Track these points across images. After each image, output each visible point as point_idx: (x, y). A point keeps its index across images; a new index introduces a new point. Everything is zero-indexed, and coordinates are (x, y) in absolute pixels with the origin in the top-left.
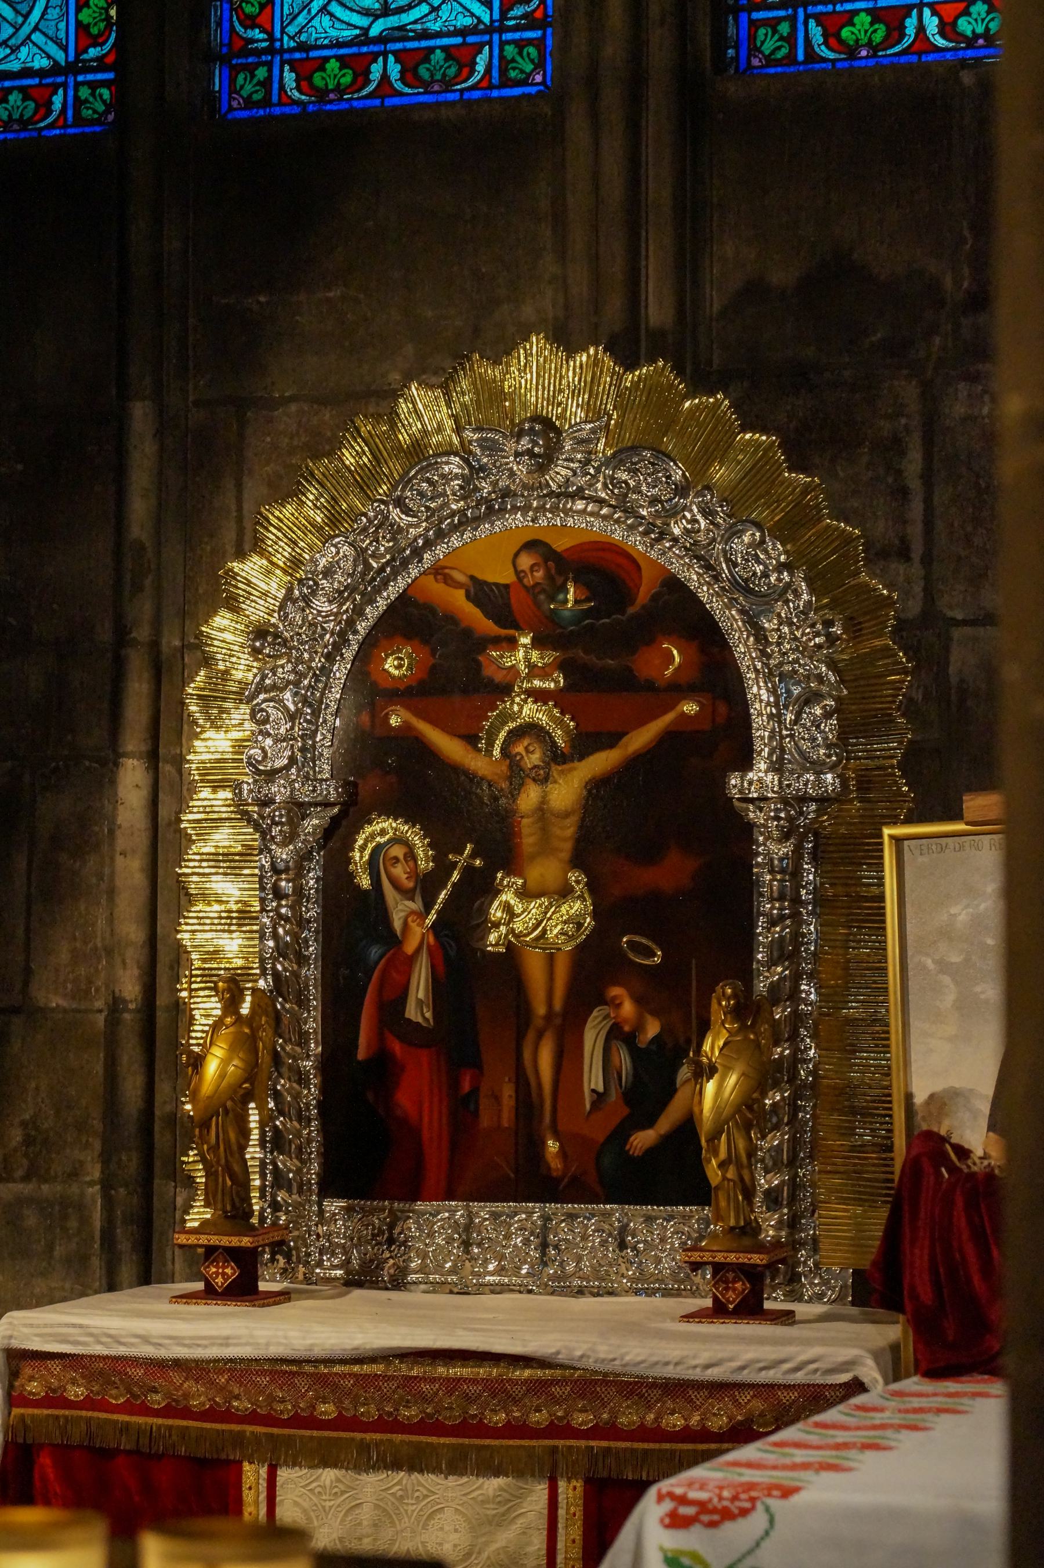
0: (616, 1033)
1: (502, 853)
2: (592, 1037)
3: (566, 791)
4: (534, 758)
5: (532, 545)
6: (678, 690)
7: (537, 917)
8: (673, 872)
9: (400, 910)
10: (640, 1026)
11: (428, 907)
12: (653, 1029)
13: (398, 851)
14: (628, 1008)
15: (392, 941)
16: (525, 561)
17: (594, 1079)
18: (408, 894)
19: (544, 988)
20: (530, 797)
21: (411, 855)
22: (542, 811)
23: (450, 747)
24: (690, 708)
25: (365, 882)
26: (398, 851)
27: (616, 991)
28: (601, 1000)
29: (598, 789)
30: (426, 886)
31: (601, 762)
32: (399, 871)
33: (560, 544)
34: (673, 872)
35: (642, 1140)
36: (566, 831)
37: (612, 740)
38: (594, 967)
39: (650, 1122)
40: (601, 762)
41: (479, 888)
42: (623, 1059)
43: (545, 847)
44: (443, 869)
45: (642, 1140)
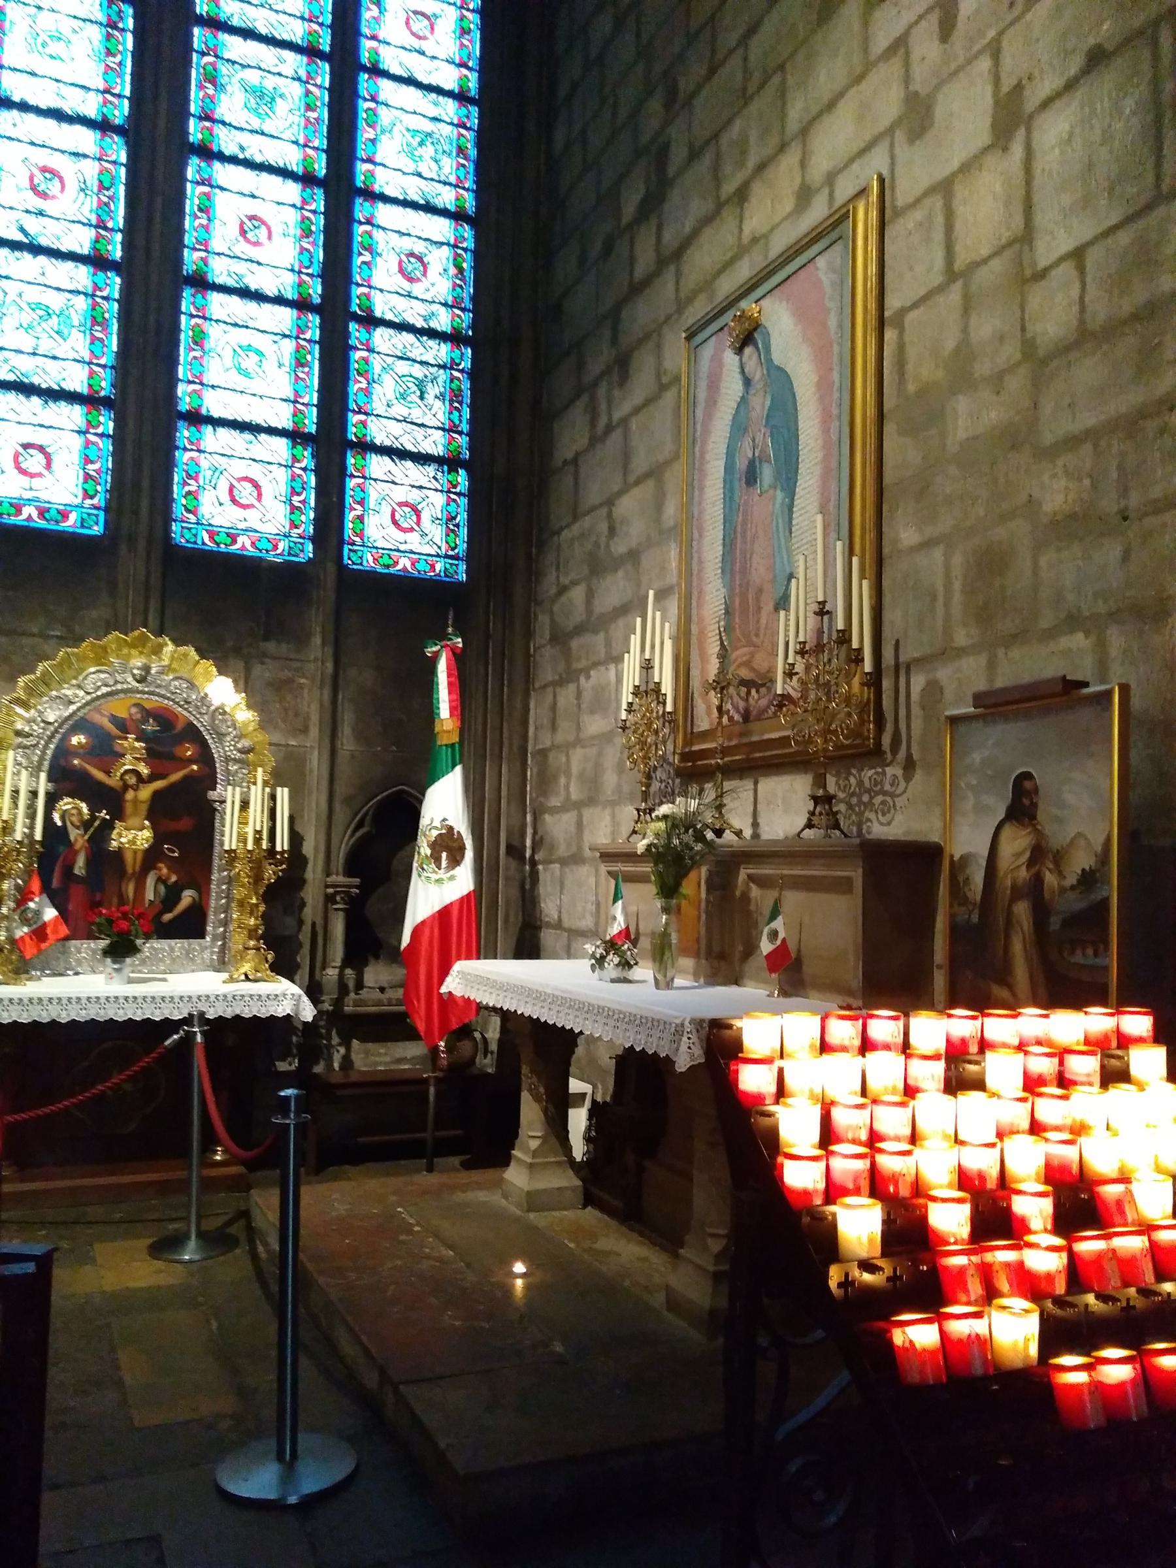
0: (160, 880)
1: (118, 813)
2: (150, 881)
3: (145, 793)
4: (132, 780)
5: (135, 705)
6: (190, 761)
7: (132, 837)
8: (185, 824)
9: (74, 834)
10: (168, 878)
11: (86, 833)
12: (174, 878)
13: (74, 812)
14: (165, 871)
15: (70, 844)
16: (134, 710)
17: (150, 895)
18: (77, 828)
19: (131, 863)
20: (130, 795)
21: (80, 812)
22: (135, 801)
23: (99, 775)
24: (195, 767)
25: (59, 823)
26: (74, 812)
27: (161, 865)
28: (155, 868)
29: (156, 794)
30: (86, 825)
31: (159, 784)
32: (74, 819)
33: (147, 706)
34: (185, 824)
35: (168, 917)
36: (144, 808)
37: (163, 776)
38: (152, 857)
39: (170, 912)
40: (159, 784)
41: (108, 826)
42: (162, 889)
43: (135, 813)
44: (93, 818)
45: (168, 917)
